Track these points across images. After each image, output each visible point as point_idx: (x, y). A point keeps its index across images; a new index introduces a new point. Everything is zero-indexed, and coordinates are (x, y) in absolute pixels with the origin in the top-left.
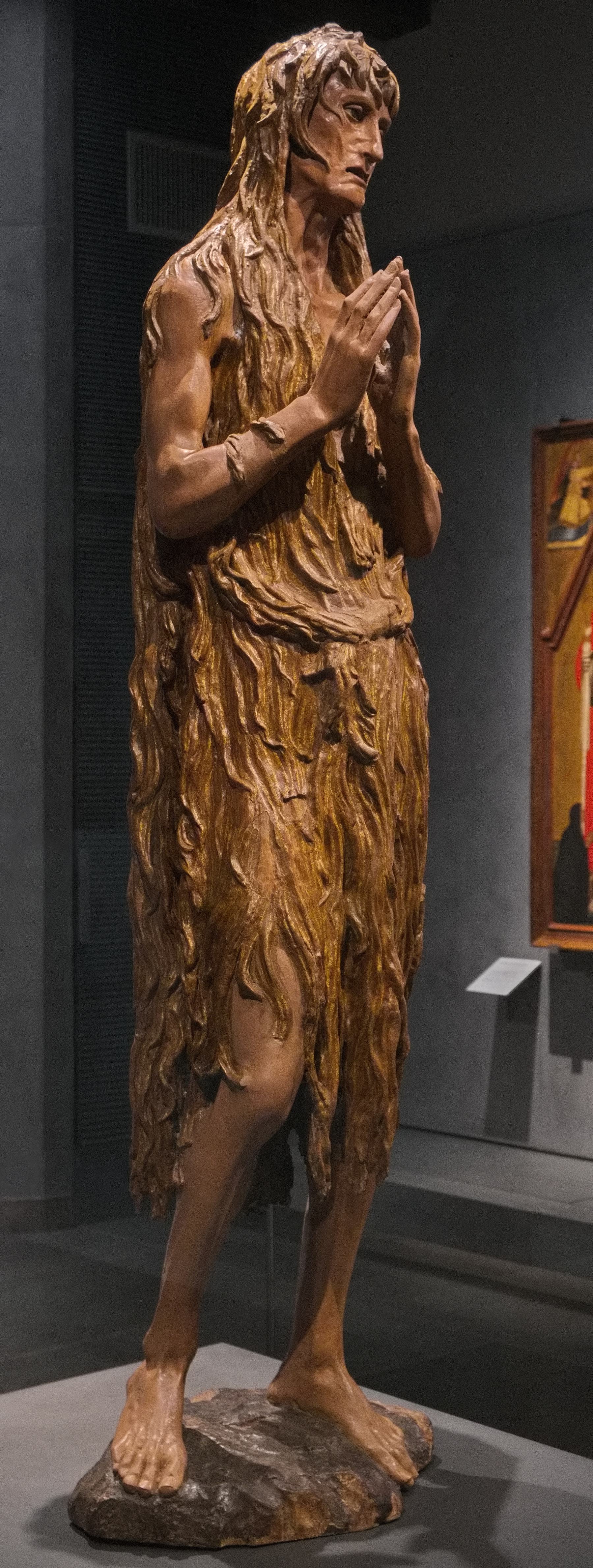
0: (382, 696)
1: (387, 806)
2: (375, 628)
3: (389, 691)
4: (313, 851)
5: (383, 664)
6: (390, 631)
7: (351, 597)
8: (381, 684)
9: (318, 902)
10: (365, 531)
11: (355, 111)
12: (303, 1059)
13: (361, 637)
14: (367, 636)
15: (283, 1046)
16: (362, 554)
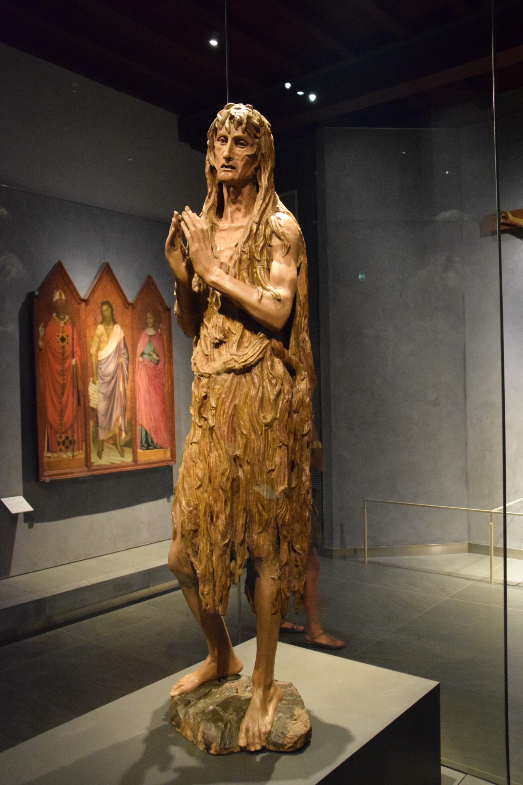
0: (220, 400)
1: (222, 449)
2: (217, 370)
3: (224, 398)
4: (195, 466)
5: (222, 385)
6: (226, 370)
7: (212, 357)
8: (220, 395)
9: (194, 487)
10: (217, 327)
11: (223, 141)
12: (184, 550)
13: (210, 375)
14: (213, 374)
15: (173, 543)
16: (213, 338)
